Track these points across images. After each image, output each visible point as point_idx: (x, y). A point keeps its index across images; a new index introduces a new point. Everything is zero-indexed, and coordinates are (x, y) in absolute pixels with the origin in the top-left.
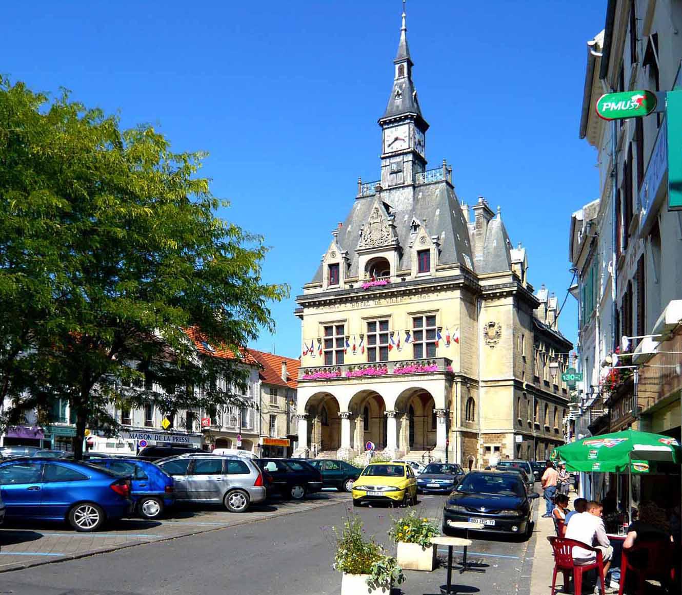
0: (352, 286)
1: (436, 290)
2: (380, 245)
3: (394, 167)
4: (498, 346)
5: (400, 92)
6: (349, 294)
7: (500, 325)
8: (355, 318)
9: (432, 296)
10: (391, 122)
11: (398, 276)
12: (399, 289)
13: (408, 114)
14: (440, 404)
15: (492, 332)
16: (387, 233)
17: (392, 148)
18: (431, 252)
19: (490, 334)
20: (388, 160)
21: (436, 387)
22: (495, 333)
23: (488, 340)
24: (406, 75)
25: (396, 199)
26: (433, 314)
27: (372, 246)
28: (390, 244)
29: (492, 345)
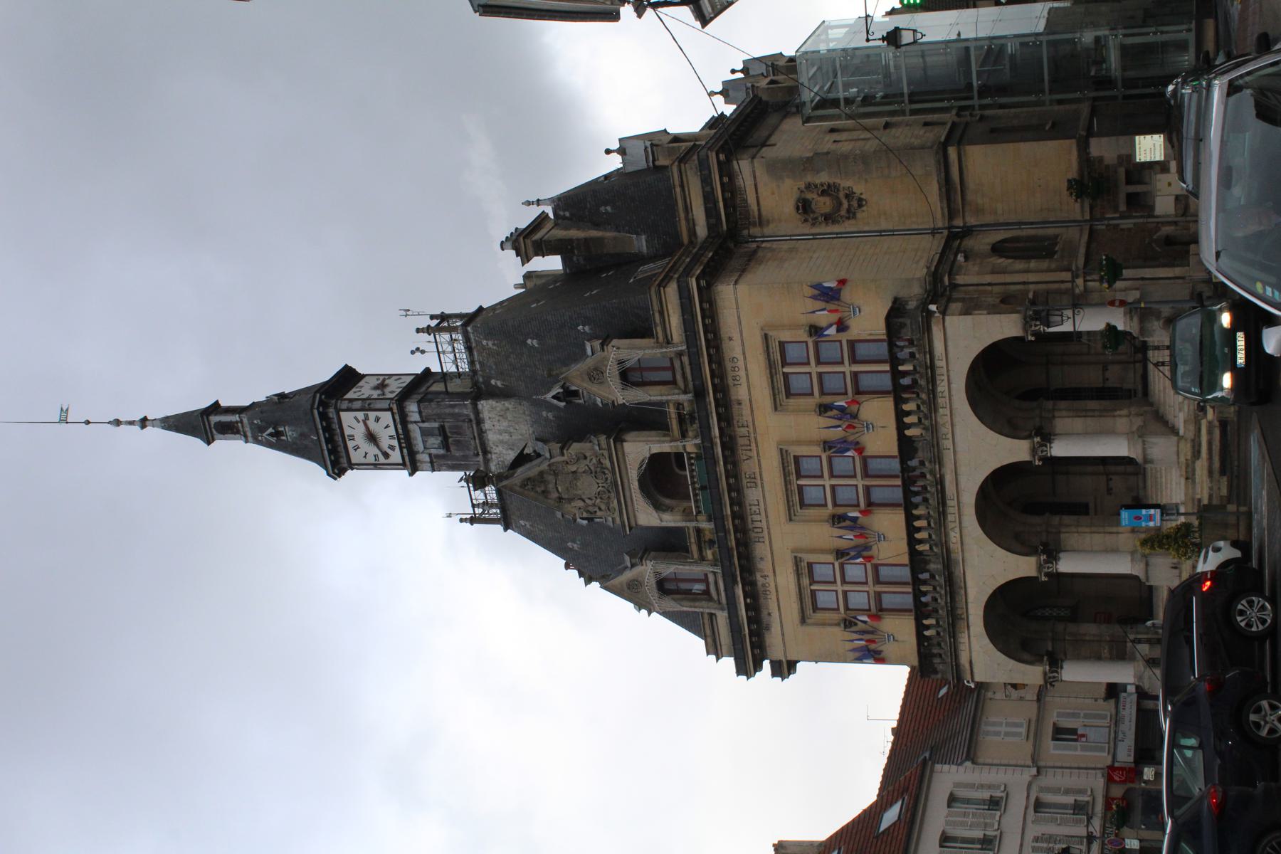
0: (711, 543)
1: (715, 342)
2: (609, 476)
3: (435, 441)
4: (858, 189)
5: (271, 430)
6: (730, 550)
7: (803, 187)
9: (733, 350)
12: (716, 432)
13: (316, 412)
14: (1007, 326)
15: (823, 204)
17: (392, 447)
18: (624, 354)
19: (827, 209)
20: (419, 457)
21: (962, 339)
22: (827, 200)
23: (843, 212)
24: (235, 418)
25: (506, 437)
26: (775, 347)
29: (855, 203)
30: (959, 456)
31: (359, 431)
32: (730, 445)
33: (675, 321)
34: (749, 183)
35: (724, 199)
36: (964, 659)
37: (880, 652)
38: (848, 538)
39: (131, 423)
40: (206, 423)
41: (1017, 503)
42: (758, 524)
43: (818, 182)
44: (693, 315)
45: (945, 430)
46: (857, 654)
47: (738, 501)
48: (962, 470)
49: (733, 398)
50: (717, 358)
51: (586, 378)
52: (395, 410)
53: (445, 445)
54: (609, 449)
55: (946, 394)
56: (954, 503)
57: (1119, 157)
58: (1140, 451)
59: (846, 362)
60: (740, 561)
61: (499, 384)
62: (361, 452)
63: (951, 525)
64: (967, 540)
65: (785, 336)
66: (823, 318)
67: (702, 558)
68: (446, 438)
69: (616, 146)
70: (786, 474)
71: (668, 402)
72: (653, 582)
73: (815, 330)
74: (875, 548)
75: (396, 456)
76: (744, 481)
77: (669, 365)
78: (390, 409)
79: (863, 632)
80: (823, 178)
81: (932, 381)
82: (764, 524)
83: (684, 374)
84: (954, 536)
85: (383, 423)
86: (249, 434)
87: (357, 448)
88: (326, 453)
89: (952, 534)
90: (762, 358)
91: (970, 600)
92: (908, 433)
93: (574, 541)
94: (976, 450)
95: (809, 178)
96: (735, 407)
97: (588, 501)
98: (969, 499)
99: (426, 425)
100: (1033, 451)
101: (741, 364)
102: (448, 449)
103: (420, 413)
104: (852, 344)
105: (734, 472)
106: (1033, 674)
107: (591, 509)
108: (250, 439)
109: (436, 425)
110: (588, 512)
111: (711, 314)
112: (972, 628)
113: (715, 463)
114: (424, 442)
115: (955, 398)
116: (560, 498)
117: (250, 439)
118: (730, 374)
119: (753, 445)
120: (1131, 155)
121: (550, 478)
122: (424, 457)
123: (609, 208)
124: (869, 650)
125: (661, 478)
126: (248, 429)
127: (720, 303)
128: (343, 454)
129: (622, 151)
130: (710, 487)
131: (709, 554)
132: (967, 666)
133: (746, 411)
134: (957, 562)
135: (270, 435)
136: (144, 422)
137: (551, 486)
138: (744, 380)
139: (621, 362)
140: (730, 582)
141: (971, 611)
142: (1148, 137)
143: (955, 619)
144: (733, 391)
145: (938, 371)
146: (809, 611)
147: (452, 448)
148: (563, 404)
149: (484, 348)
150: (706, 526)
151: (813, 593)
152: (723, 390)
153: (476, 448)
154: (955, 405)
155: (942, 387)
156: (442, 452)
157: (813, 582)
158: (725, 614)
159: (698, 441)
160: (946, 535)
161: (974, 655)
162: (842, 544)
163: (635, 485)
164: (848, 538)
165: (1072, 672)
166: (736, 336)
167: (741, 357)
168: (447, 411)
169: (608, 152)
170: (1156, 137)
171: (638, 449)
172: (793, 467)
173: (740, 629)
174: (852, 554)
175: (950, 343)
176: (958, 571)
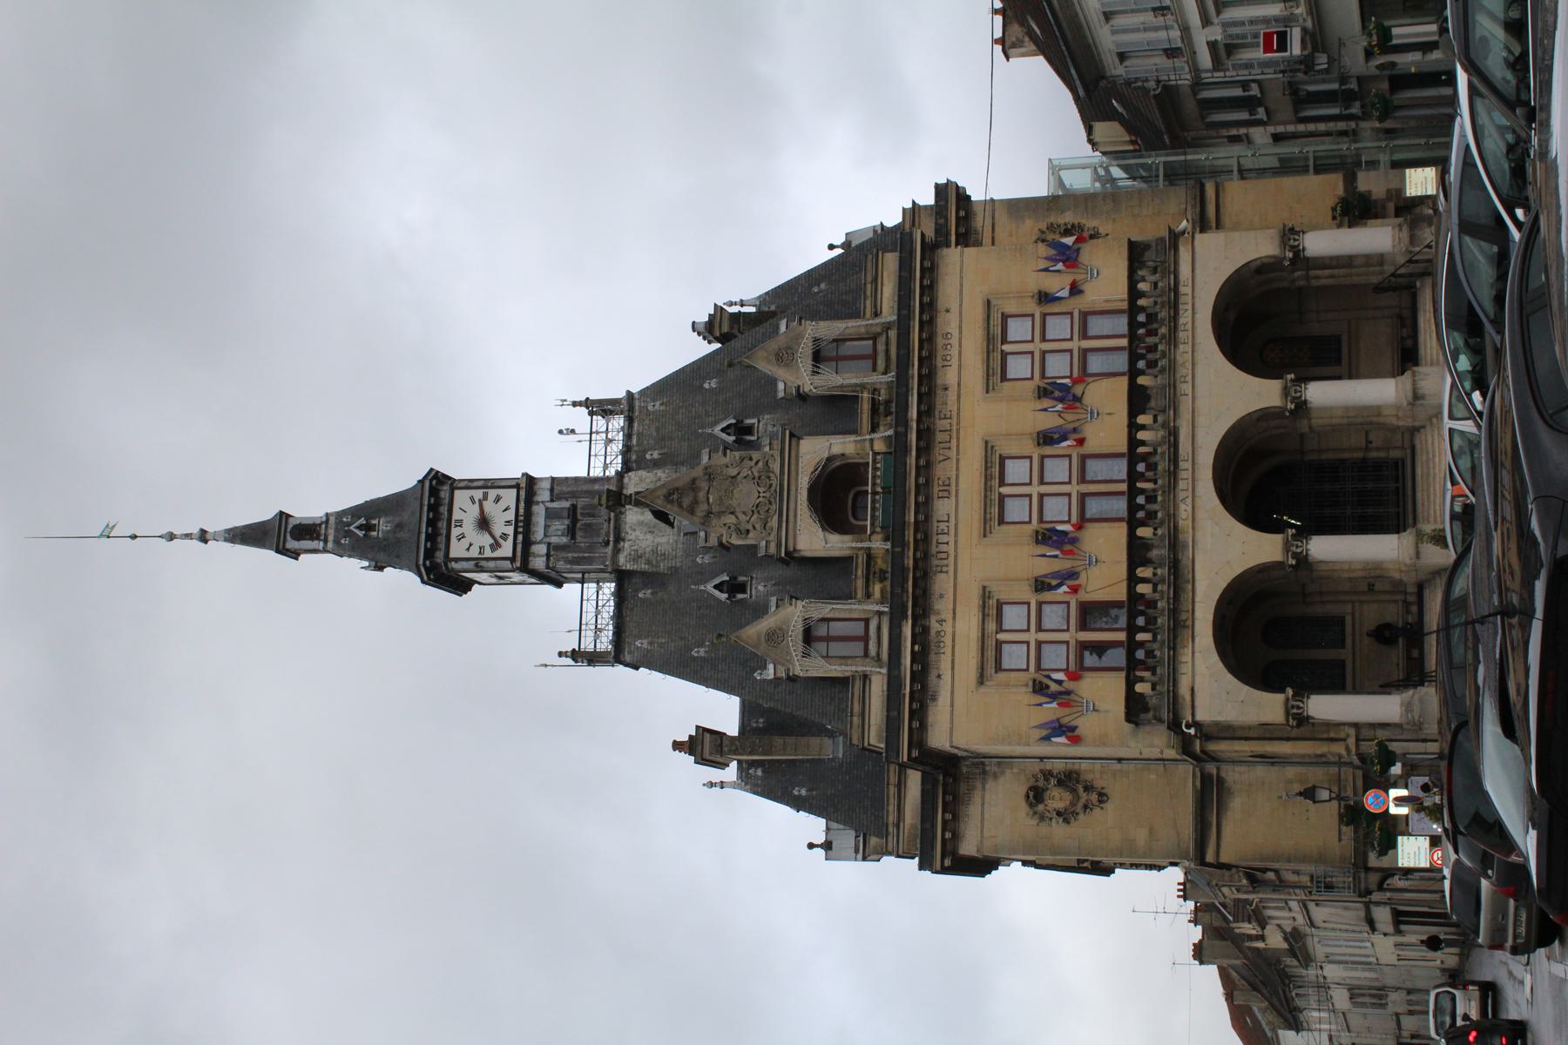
1: (929, 307)
2: (775, 482)
3: (560, 525)
5: (362, 521)
6: (904, 570)
7: (1044, 227)
9: (948, 323)
10: (432, 537)
12: (913, 413)
14: (1263, 246)
16: (747, 463)
26: (996, 319)
27: (774, 507)
28: (777, 454)
30: (1200, 403)
31: (474, 511)
32: (926, 434)
33: (889, 290)
34: (988, 222)
35: (957, 235)
36: (1184, 690)
37: (1073, 729)
38: (1047, 563)
39: (188, 536)
40: (283, 535)
41: (1263, 476)
42: (943, 548)
43: (1061, 221)
44: (911, 271)
45: (1184, 371)
46: (1044, 733)
47: (925, 507)
48: (1201, 420)
49: (939, 381)
50: (928, 325)
51: (773, 358)
52: (523, 485)
53: (571, 531)
54: (783, 442)
55: (1189, 326)
56: (1188, 465)
57: (1388, 191)
58: (1409, 387)
59: (1076, 337)
61: (656, 455)
62: (465, 543)
63: (1181, 495)
64: (1200, 515)
65: (1010, 308)
66: (1058, 284)
67: (868, 595)
68: (574, 520)
69: (840, 239)
70: (988, 478)
71: (863, 386)
72: (800, 628)
73: (1044, 298)
74: (1083, 575)
75: (506, 549)
76: (936, 489)
77: (869, 351)
78: (517, 487)
79: (1053, 697)
80: (1068, 218)
81: (1175, 306)
82: (951, 549)
83: (887, 351)
84: (1184, 510)
85: (502, 504)
86: (331, 538)
87: (461, 537)
88: (423, 536)
89: (1182, 507)
90: (979, 333)
91: (1197, 599)
92: (1141, 380)
93: (701, 645)
94: (1221, 397)
95: (1052, 219)
96: (939, 392)
97: (743, 518)
98: (1206, 458)
99: (555, 505)
100: (1286, 392)
101: (954, 341)
102: (573, 537)
103: (552, 490)
104: (1085, 316)
105: (925, 469)
106: (1269, 707)
107: (744, 526)
108: (330, 545)
109: (566, 504)
110: (739, 531)
111: (930, 289)
112: (1197, 640)
114: (546, 527)
115: (1198, 331)
116: (709, 513)
117: (330, 545)
119: (954, 442)
120: (1400, 190)
121: (704, 485)
122: (540, 549)
123: (823, 286)
124: (1061, 726)
125: (836, 495)
126: (331, 532)
127: (942, 270)
128: (442, 546)
129: (846, 245)
130: (895, 491)
131: (877, 589)
132: (1188, 697)
133: (952, 396)
134: (1185, 546)
135: (360, 527)
136: (203, 537)
137: (701, 495)
138: (955, 362)
139: (816, 340)
141: (1198, 614)
142: (1419, 170)
143: (1179, 625)
144: (940, 373)
145: (1182, 299)
146: (990, 669)
147: (579, 539)
148: (733, 438)
149: (648, 413)
150: (878, 545)
151: (999, 645)
152: (928, 377)
153: (608, 535)
154: (1198, 340)
155: (1185, 318)
156: (564, 540)
157: (1000, 629)
158: (884, 671)
159: (890, 432)
160: (1176, 507)
161: (1197, 678)
162: (1043, 567)
163: (803, 495)
164: (1047, 563)
165: (1323, 706)
166: (955, 307)
167: (956, 333)
168: (585, 487)
169: (831, 247)
170: (1428, 170)
171: (815, 450)
172: (995, 465)
174: (1054, 583)
175: (1197, 265)
176: (1185, 561)
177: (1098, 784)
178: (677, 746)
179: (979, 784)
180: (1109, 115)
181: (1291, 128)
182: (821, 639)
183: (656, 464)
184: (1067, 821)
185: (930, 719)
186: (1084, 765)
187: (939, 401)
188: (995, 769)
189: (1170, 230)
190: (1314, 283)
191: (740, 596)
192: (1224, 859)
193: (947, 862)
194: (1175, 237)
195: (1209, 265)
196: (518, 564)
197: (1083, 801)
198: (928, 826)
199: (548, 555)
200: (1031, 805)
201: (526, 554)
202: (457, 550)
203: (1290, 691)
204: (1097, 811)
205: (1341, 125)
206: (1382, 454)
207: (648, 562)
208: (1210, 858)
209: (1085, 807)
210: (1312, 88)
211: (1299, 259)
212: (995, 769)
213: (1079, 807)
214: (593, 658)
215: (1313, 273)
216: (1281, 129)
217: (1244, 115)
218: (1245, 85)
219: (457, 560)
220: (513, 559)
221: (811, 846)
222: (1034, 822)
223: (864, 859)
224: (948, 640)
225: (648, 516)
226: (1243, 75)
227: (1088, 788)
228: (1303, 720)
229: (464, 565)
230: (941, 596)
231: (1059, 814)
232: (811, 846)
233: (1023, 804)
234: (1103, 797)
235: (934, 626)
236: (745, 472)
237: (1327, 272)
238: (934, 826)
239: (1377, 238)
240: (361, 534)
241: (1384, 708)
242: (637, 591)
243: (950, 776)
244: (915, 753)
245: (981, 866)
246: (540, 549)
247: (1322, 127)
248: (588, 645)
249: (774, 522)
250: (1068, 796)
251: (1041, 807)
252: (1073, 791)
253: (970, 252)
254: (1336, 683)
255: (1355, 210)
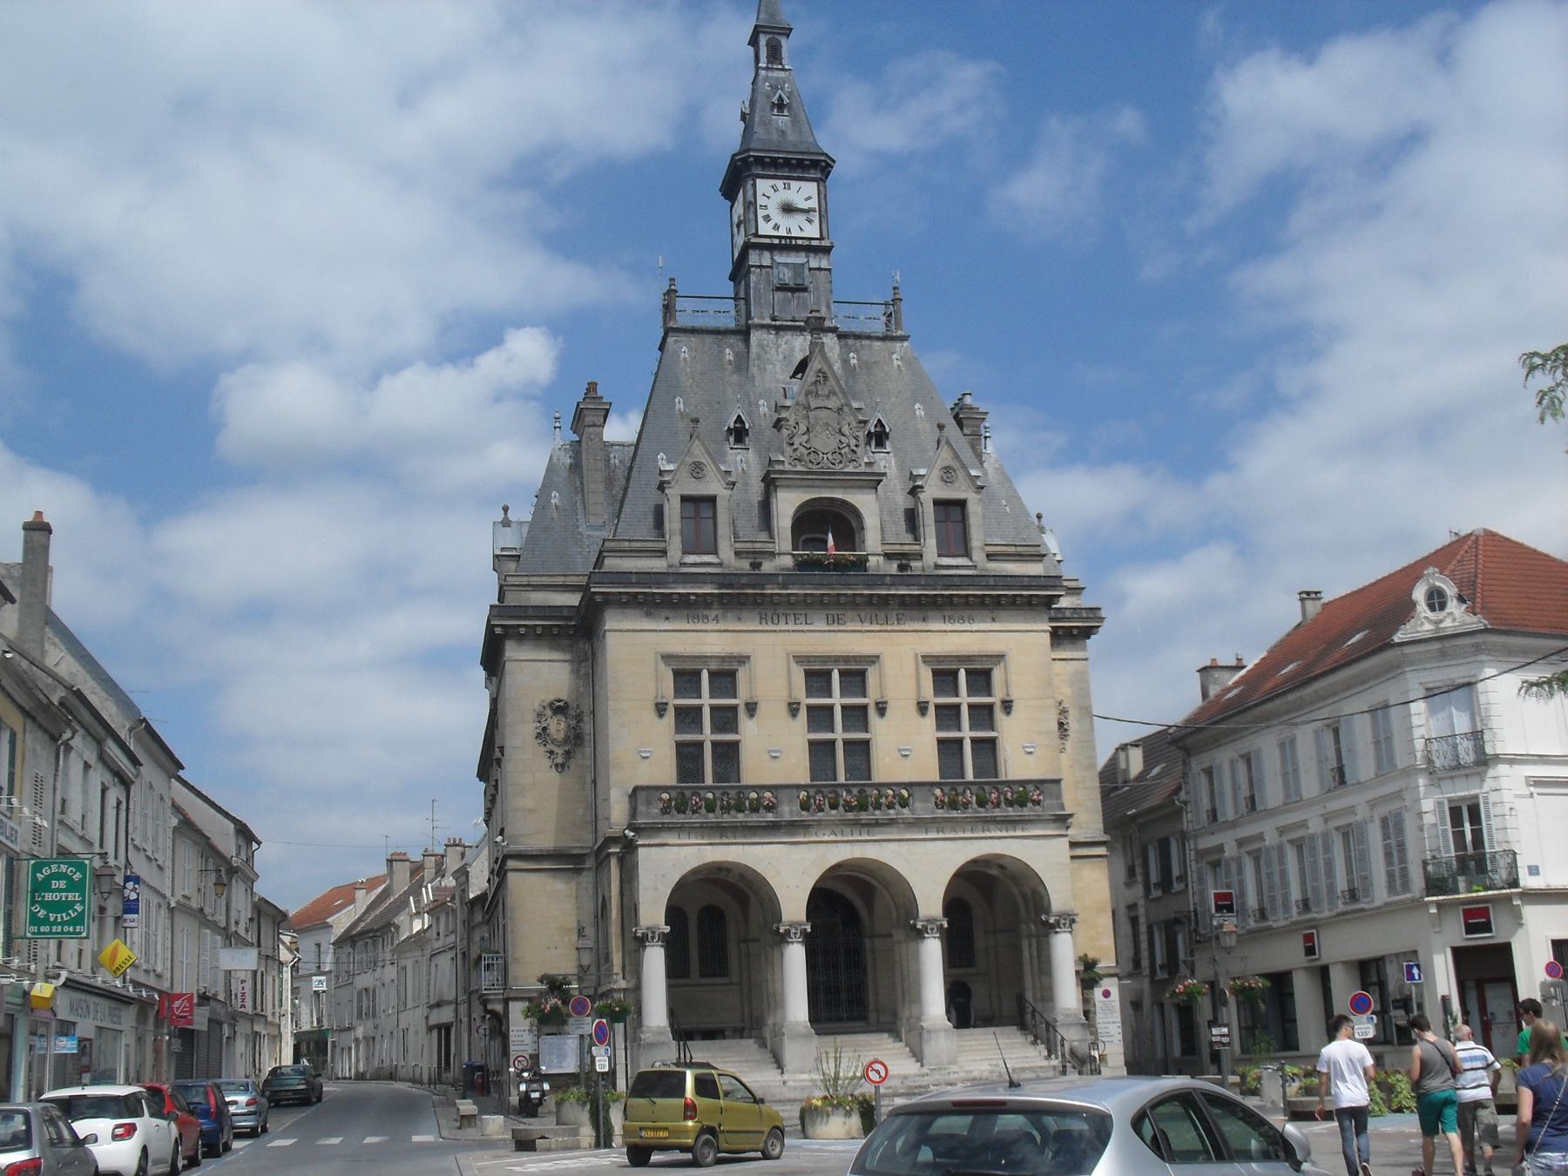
2: (838, 468)
3: (787, 276)
5: (786, 101)
8: (772, 654)
10: (774, 163)
11: (889, 556)
14: (1059, 898)
16: (853, 442)
17: (776, 227)
20: (767, 254)
27: (814, 468)
48: (905, 845)
52: (824, 243)
53: (783, 288)
60: (742, 596)
62: (770, 192)
70: (847, 659)
78: (821, 238)
85: (805, 225)
97: (805, 438)
100: (930, 920)
103: (820, 269)
113: (869, 586)
114: (786, 265)
118: (956, 614)
140: (724, 580)
165: (655, 960)
169: (1039, 517)
173: (659, 585)
177: (572, 763)
178: (592, 387)
179: (568, 657)
180: (1149, 763)
181: (1142, 920)
182: (697, 513)
183: (846, 362)
184: (538, 736)
185: (628, 612)
186: (588, 751)
187: (914, 613)
188: (583, 671)
189: (1071, 816)
190: (1025, 943)
191: (732, 439)
192: (510, 875)
193: (498, 631)
194: (1063, 820)
195: (1040, 853)
196: (754, 240)
197: (556, 750)
198: (530, 612)
199: (761, 267)
200: (551, 704)
201: (762, 247)
202: (763, 185)
203: (667, 929)
204: (548, 763)
205: (1145, 963)
206: (872, 1007)
207: (759, 357)
208: (511, 864)
209: (551, 752)
210: (1180, 938)
211: (1050, 928)
212: (583, 671)
213: (550, 747)
214: (668, 309)
215: (1034, 940)
216: (1141, 911)
217: (1154, 878)
218: (1183, 878)
219: (754, 185)
220: (756, 235)
221: (506, 509)
222: (537, 706)
223: (496, 557)
224: (700, 626)
225: (799, 357)
226: (1192, 877)
227: (568, 754)
228: (642, 942)
229: (750, 192)
230: (739, 619)
231: (545, 729)
232: (506, 509)
233: (552, 697)
234: (560, 768)
235: (713, 614)
236: (844, 439)
237: (1035, 953)
238: (530, 618)
239: (1067, 994)
240: (775, 100)
241: (656, 1012)
242: (731, 346)
243: (578, 632)
244: (598, 599)
245: (492, 660)
246: (766, 261)
247: (1144, 946)
248: (680, 304)
249: (799, 468)
250: (561, 736)
251: (549, 712)
252: (566, 740)
253: (1047, 638)
254: (676, 970)
255: (1088, 976)
